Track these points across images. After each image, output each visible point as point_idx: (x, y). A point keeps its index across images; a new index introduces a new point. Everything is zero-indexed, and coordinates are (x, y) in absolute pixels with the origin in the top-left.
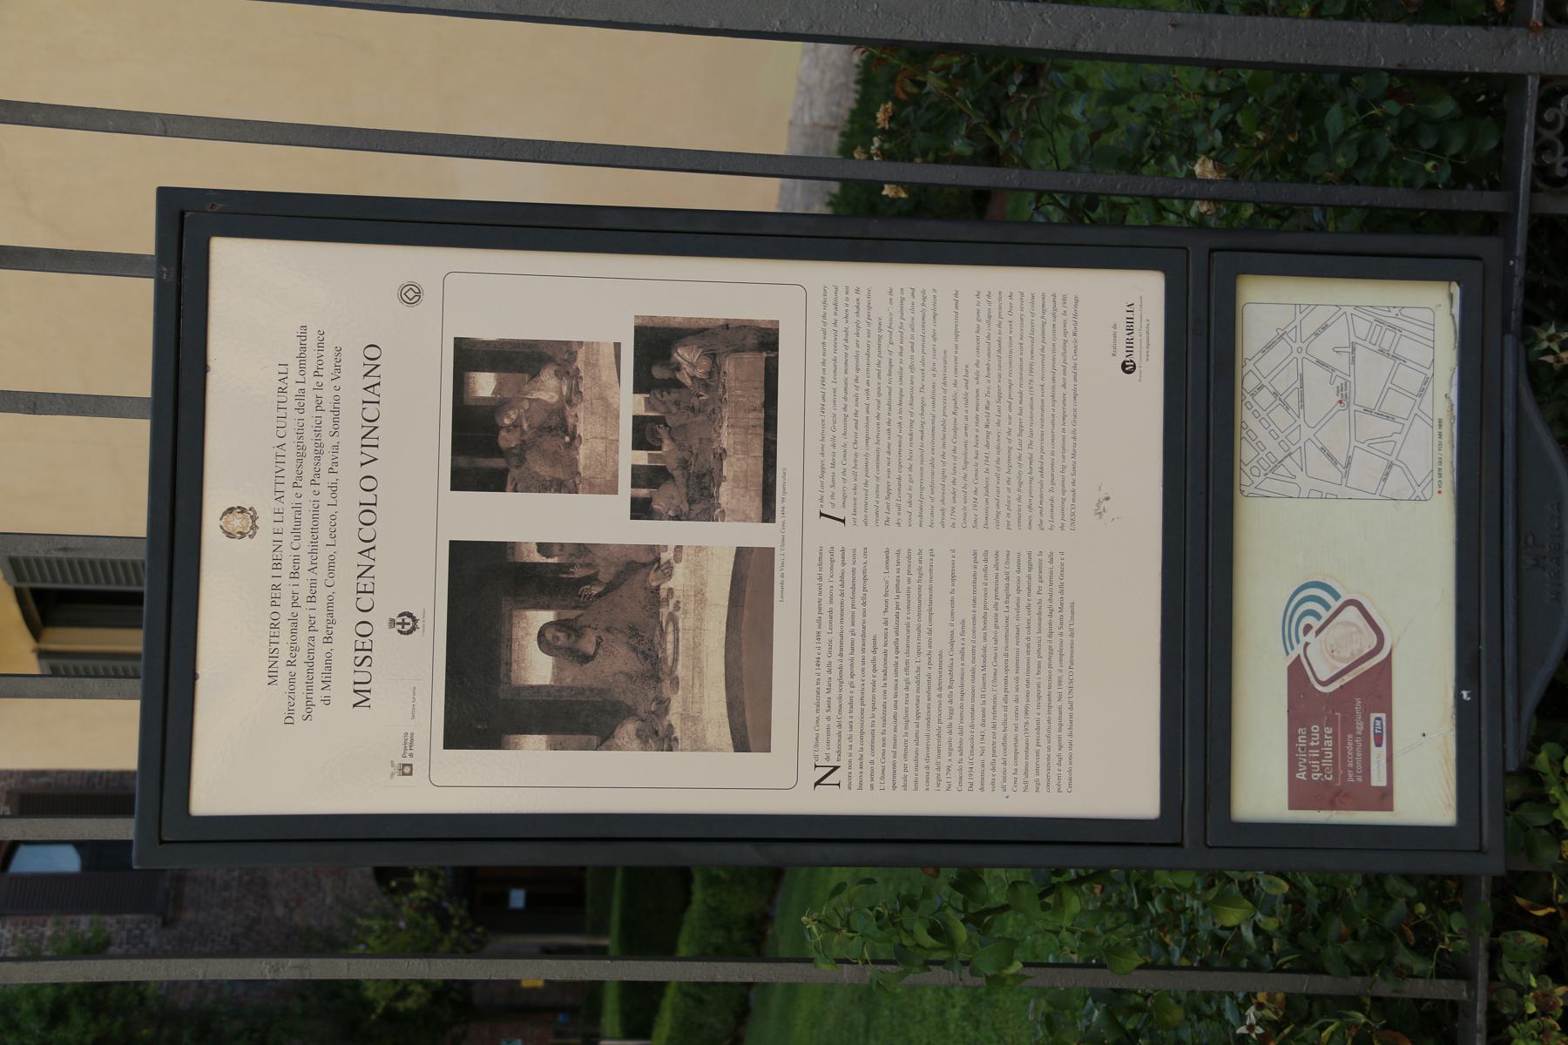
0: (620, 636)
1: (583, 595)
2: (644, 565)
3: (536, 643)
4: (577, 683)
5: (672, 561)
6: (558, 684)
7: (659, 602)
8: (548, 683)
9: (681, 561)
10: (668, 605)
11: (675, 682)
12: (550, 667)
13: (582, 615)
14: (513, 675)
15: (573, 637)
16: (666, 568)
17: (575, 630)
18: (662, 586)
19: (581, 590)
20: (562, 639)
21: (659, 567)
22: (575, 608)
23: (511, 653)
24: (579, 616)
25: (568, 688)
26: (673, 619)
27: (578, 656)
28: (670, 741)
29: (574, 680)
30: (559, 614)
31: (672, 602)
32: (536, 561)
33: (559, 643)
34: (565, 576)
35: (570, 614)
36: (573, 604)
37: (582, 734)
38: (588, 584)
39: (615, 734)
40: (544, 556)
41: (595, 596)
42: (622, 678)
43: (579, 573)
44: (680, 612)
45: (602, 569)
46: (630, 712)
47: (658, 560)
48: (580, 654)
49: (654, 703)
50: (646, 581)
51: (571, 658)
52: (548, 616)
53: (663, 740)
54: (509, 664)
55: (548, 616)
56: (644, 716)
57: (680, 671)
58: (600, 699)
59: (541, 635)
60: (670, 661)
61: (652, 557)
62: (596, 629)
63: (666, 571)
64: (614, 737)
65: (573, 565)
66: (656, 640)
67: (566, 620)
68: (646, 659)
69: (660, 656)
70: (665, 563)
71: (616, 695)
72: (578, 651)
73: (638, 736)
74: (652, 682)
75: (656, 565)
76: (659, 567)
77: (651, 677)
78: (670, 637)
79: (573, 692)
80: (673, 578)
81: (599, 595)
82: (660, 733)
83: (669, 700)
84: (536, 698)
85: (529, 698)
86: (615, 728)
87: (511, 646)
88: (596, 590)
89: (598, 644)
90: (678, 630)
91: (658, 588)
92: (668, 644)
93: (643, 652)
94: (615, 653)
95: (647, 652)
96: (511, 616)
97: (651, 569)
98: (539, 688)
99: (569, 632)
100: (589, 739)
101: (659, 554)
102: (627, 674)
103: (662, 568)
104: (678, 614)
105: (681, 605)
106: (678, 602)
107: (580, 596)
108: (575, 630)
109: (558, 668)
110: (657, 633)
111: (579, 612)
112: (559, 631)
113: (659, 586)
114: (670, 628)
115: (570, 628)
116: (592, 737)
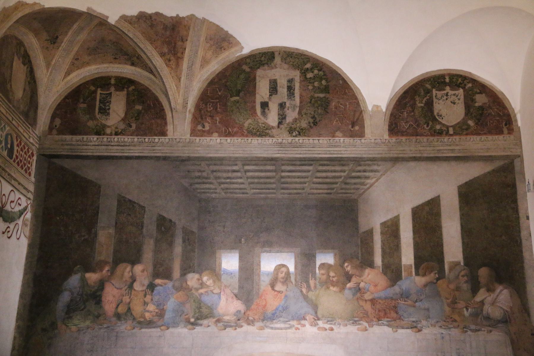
0: (283, 302)
1: (302, 284)
2: (316, 313)
3: (280, 263)
4: (262, 283)
5: (318, 326)
6: (261, 274)
7: (299, 320)
8: (262, 269)
9: (318, 330)
10: (298, 324)
11: (262, 328)
12: (269, 270)
13: (293, 284)
14: (265, 254)
15: (282, 280)
16: (315, 324)
17: (285, 281)
18: (306, 321)
19: (304, 283)
20: (281, 275)
21: (315, 320)
22: (296, 280)
23: (275, 253)
24: (292, 283)
25: (260, 278)
26: (291, 327)
27: (273, 283)
28: (235, 326)
29: (264, 281)
30: (293, 274)
31: (299, 326)
32: (317, 263)
33: (280, 274)
34: (310, 276)
35: (293, 279)
36: (297, 280)
37: (239, 286)
38: (307, 287)
39: (239, 300)
40: (319, 266)
41: (301, 290)
42: (264, 303)
43: (312, 282)
44: (295, 331)
45: (314, 293)
46: (248, 308)
47: (319, 319)
48: (275, 283)
49: (252, 319)
50: (308, 314)
51: (273, 279)
52: (292, 269)
53: (236, 323)
54: (270, 252)
55: (292, 269)
56: (247, 314)
57: (267, 331)
58: (254, 293)
59: (283, 266)
60: (272, 326)
61: (320, 316)
62: (286, 290)
63: (313, 323)
64: (237, 300)
65: (315, 279)
66: (281, 319)
67: (290, 277)
68: (272, 314)
69: (274, 321)
70: (317, 323)
71: (256, 301)
72: (277, 283)
73: (237, 312)
74: (262, 318)
75: (316, 318)
76: (315, 320)
77: (264, 318)
78: (282, 325)
79: (257, 280)
80: (310, 327)
81: (301, 291)
82: (239, 322)
83: (254, 325)
84: (255, 264)
85: (255, 261)
86: (241, 300)
87: (278, 252)
88: (304, 291)
89: (279, 292)
90: (286, 329)
91: (305, 319)
92: (279, 325)
93: (276, 313)
94: (275, 300)
95: (276, 315)
96: (291, 252)
97: (315, 316)
98: (259, 265)
99: (285, 279)
100: (236, 289)
101: (322, 320)
102: (265, 306)
103: (315, 322)
104: (294, 329)
105: (298, 331)
106: (299, 329)
107: (301, 283)
108: (285, 281)
109: (268, 274)
110: (285, 320)
111: (294, 284)
112: (285, 273)
113: (306, 320)
114: (287, 326)
115: (287, 279)
116: (237, 290)
